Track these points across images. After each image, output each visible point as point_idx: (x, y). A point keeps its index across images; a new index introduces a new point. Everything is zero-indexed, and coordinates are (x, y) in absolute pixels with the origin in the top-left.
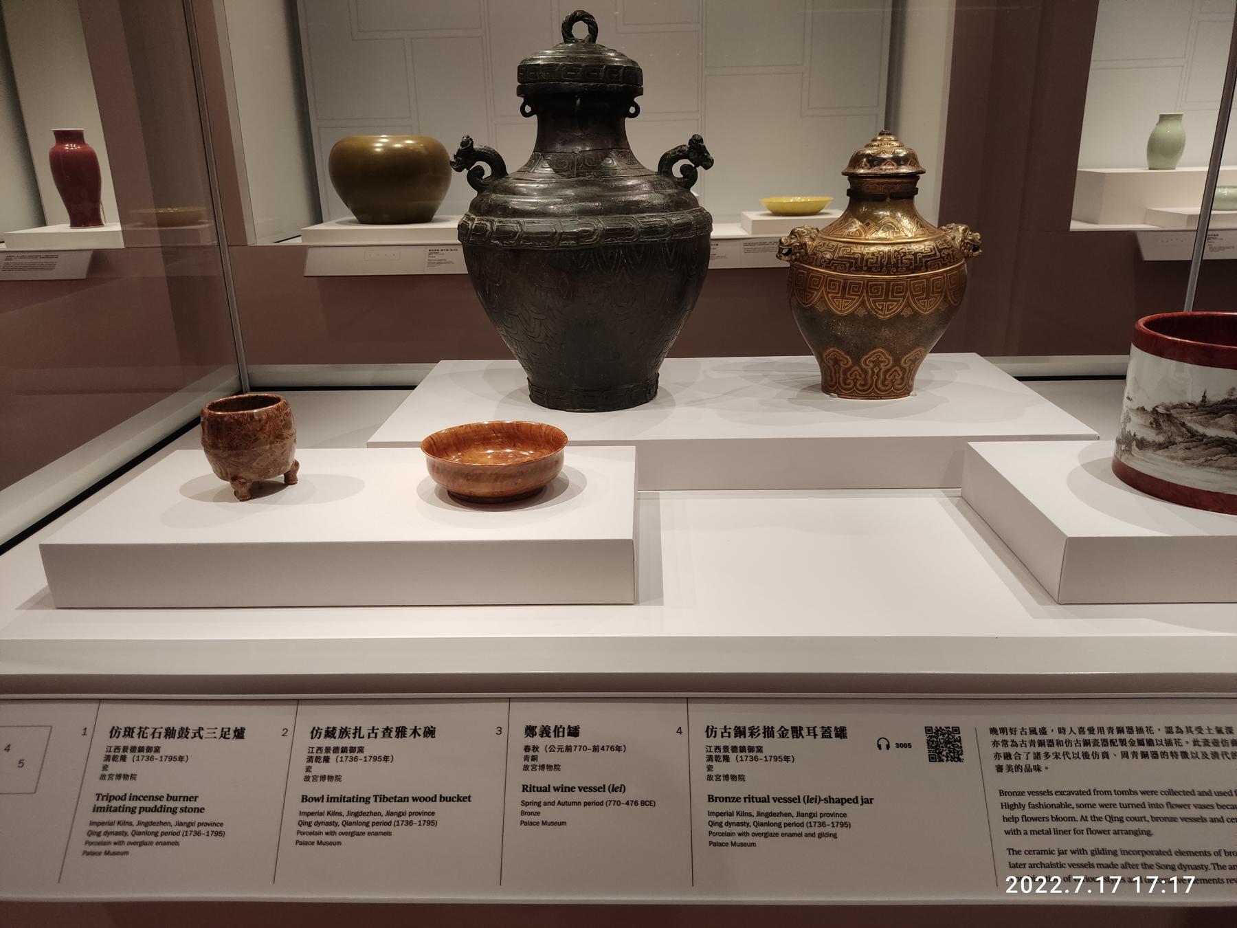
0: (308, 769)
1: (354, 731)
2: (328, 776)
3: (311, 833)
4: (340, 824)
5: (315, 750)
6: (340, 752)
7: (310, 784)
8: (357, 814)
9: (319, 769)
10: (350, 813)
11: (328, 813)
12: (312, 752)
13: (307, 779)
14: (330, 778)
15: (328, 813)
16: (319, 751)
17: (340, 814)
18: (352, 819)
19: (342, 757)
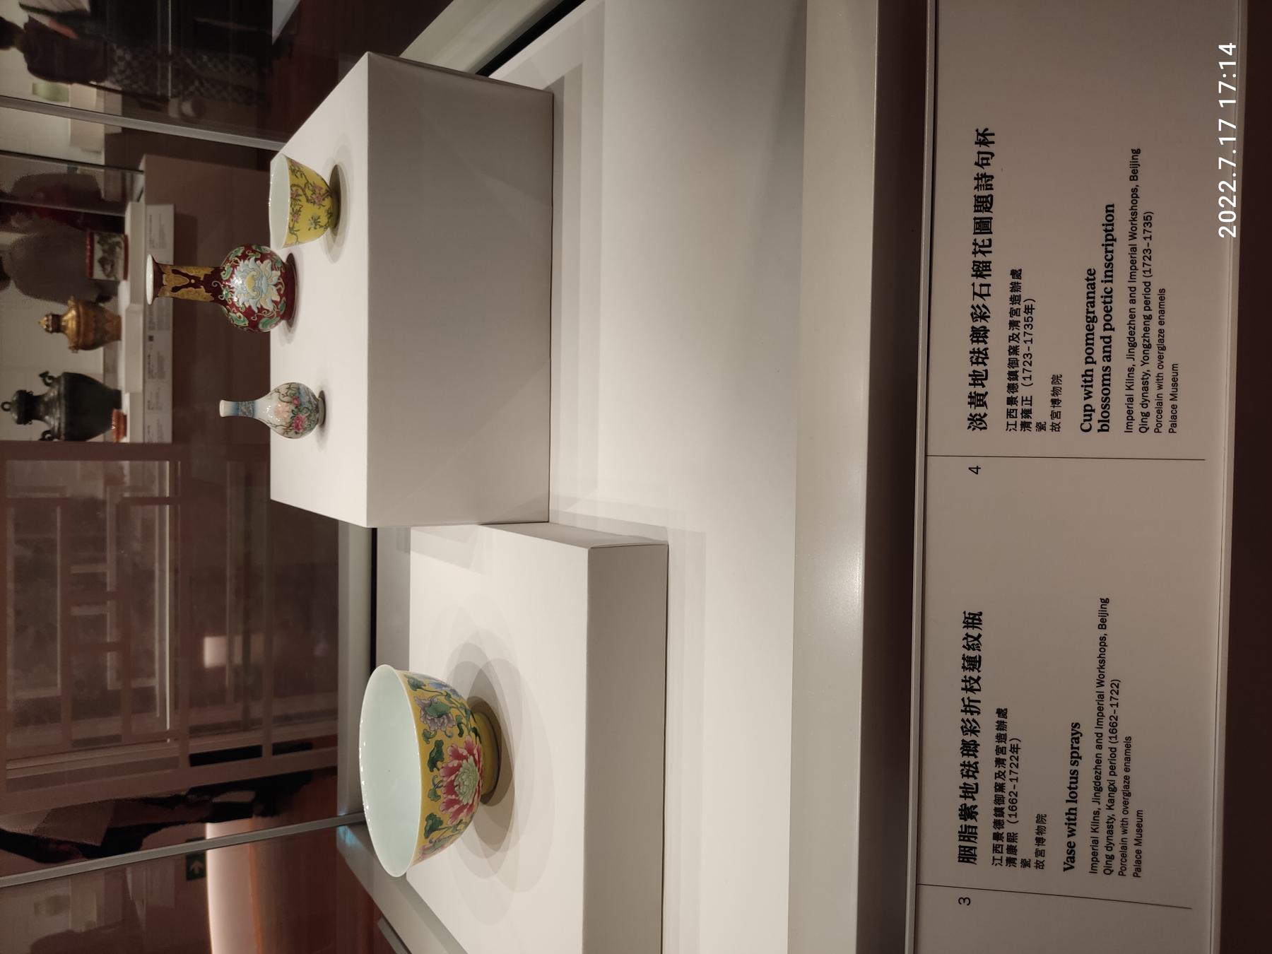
0: (1025, 864)
1: (969, 714)
2: (1038, 833)
3: (1124, 856)
4: (1110, 813)
5: (998, 856)
6: (1001, 818)
7: (1048, 859)
8: (1098, 789)
9: (1026, 848)
10: (1096, 799)
11: (1094, 831)
12: (1001, 860)
13: (1040, 865)
14: (1040, 830)
15: (1094, 831)
16: (1000, 849)
17: (1097, 813)
18: (1104, 795)
19: (1010, 815)
